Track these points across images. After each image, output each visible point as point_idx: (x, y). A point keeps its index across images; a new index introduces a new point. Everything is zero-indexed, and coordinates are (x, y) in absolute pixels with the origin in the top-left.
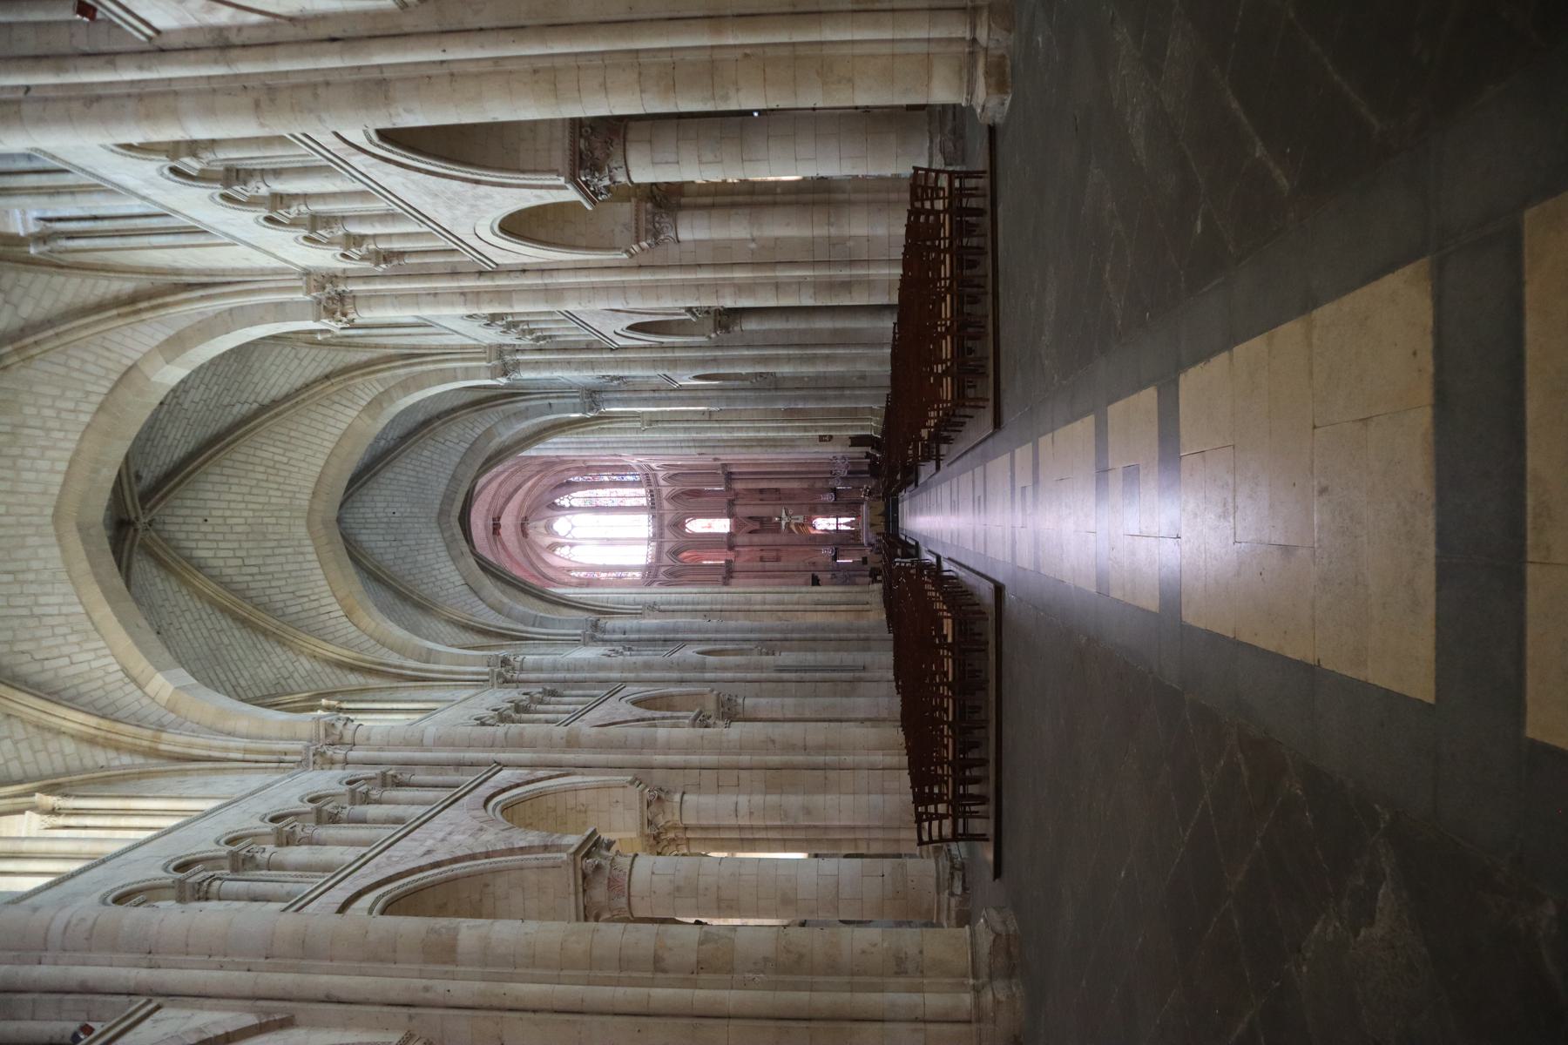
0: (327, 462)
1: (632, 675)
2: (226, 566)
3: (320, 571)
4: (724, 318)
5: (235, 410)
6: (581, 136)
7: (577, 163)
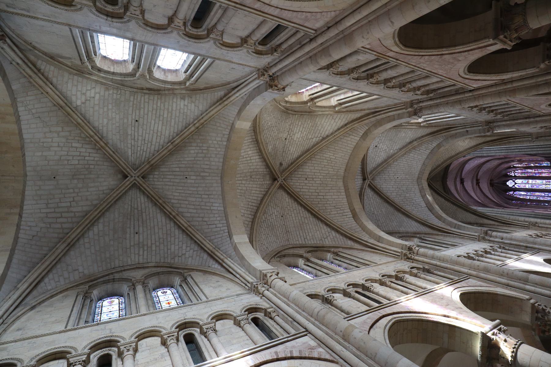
0: (349, 158)
1: (474, 273)
2: (312, 195)
3: (346, 199)
5: (314, 140)
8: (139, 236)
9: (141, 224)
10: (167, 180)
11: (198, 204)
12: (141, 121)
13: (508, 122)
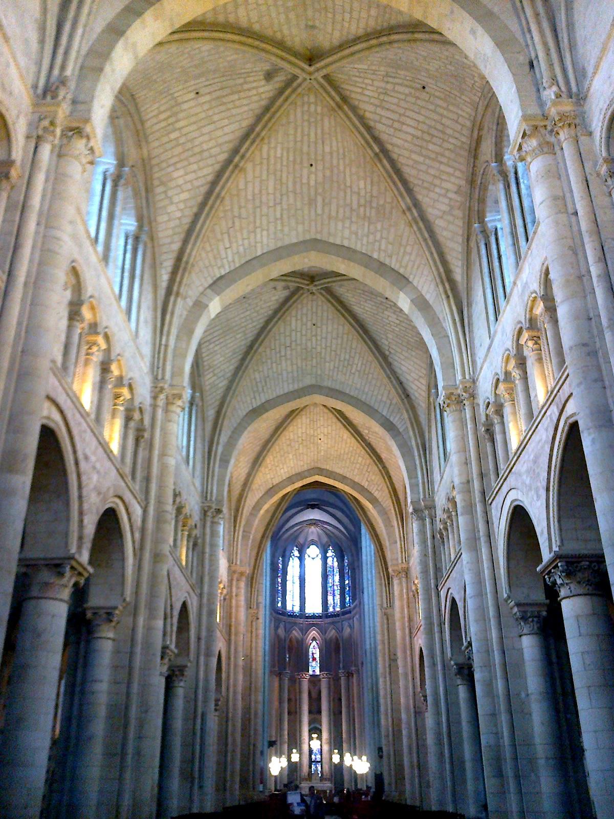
0: (352, 397)
3: (282, 393)
4: (466, 672)
5: (383, 341)
6: (591, 562)
7: (570, 560)
8: (193, 99)
9: (214, 95)
10: (306, 129)
11: (264, 199)
12: (424, 95)
13: (405, 596)
